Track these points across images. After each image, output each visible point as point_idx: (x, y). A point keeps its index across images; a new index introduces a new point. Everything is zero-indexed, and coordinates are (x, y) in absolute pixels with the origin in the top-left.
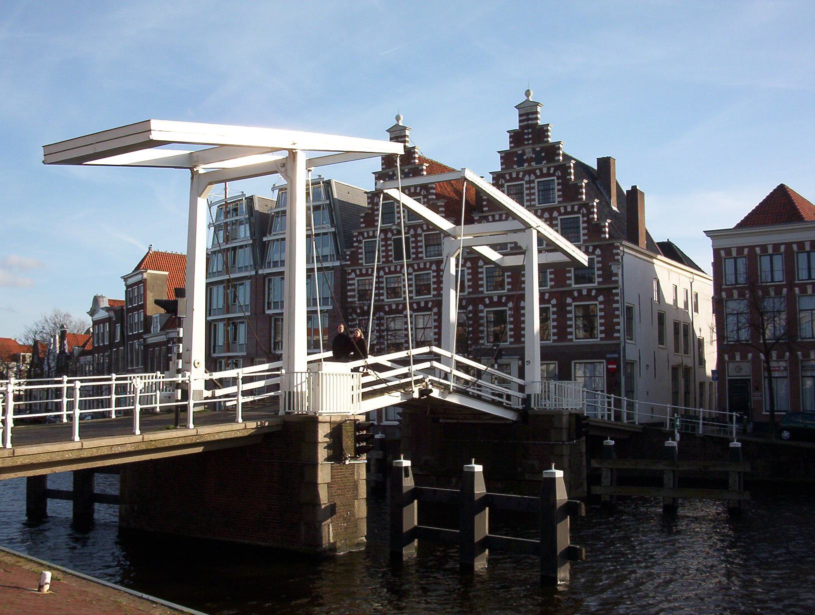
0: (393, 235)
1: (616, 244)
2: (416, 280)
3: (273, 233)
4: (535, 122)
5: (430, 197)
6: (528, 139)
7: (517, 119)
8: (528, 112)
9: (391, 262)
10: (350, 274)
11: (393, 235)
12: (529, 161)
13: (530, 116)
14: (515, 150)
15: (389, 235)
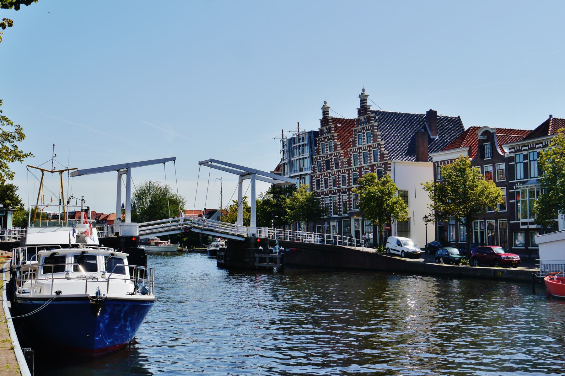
0: (325, 158)
1: (388, 162)
2: (342, 178)
3: (294, 156)
4: (366, 104)
5: (335, 140)
6: (362, 113)
7: (359, 103)
8: (363, 99)
9: (334, 169)
10: (313, 177)
11: (325, 158)
12: (363, 123)
13: (363, 102)
14: (359, 118)
15: (324, 159)
